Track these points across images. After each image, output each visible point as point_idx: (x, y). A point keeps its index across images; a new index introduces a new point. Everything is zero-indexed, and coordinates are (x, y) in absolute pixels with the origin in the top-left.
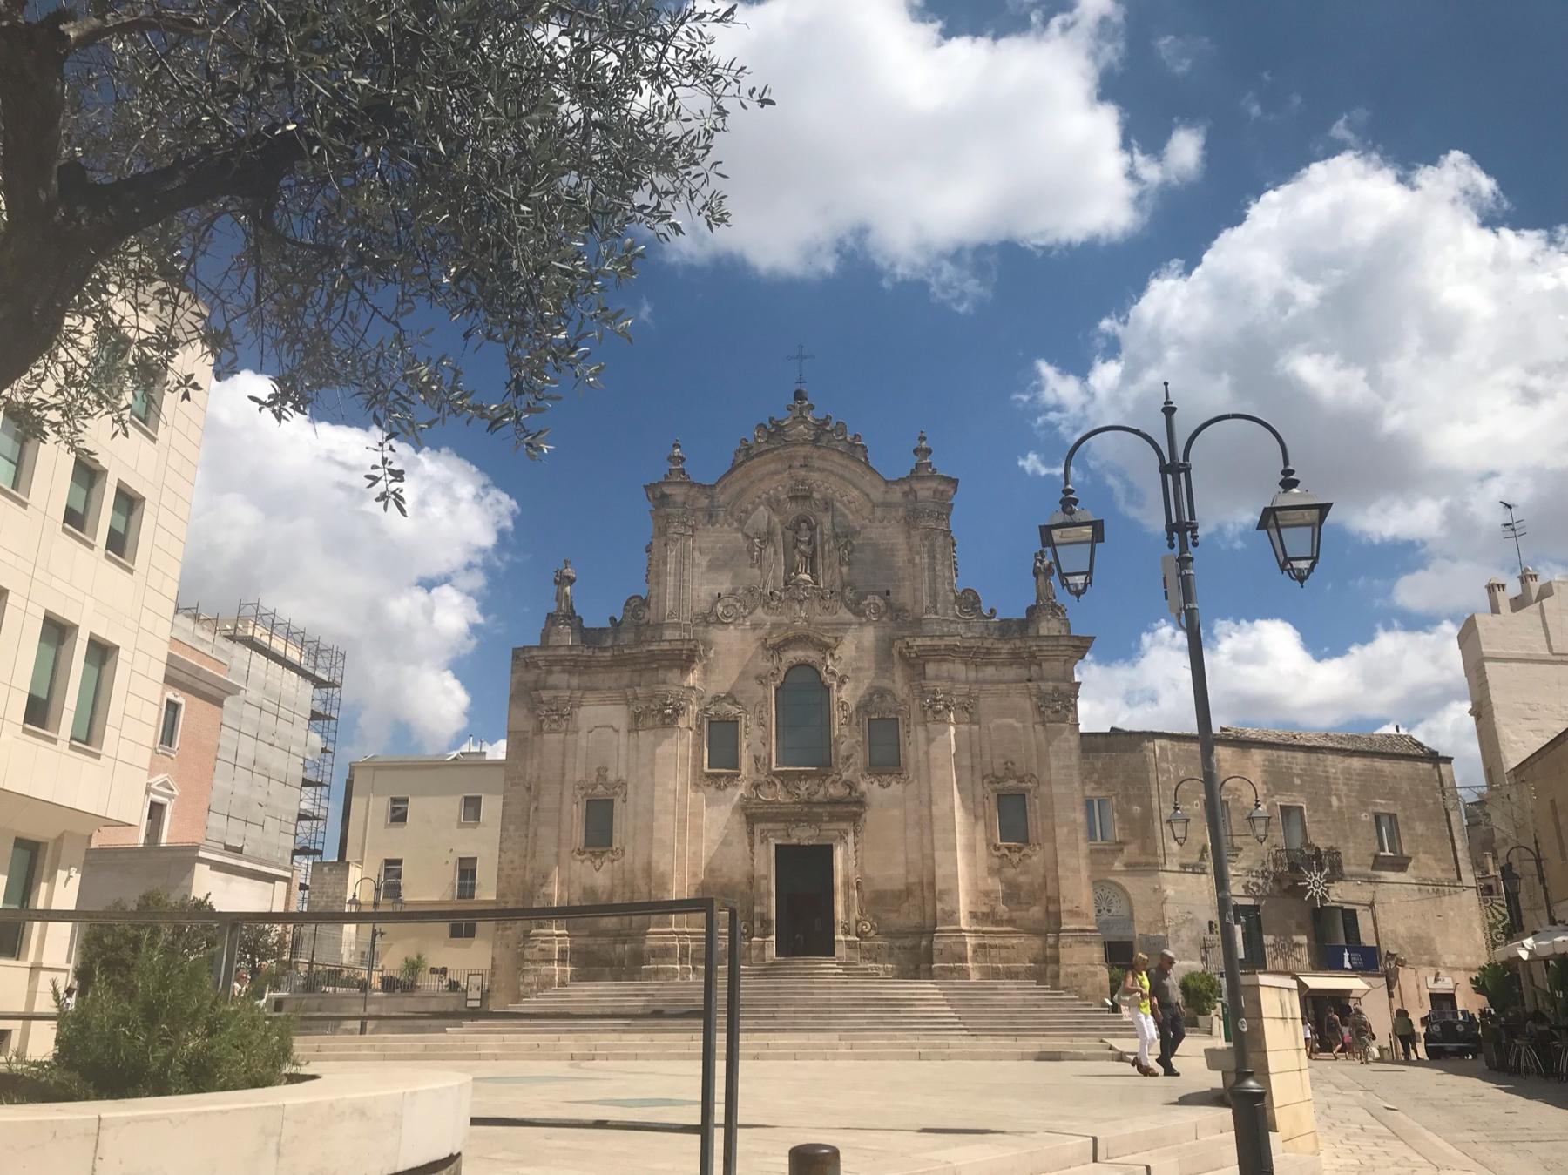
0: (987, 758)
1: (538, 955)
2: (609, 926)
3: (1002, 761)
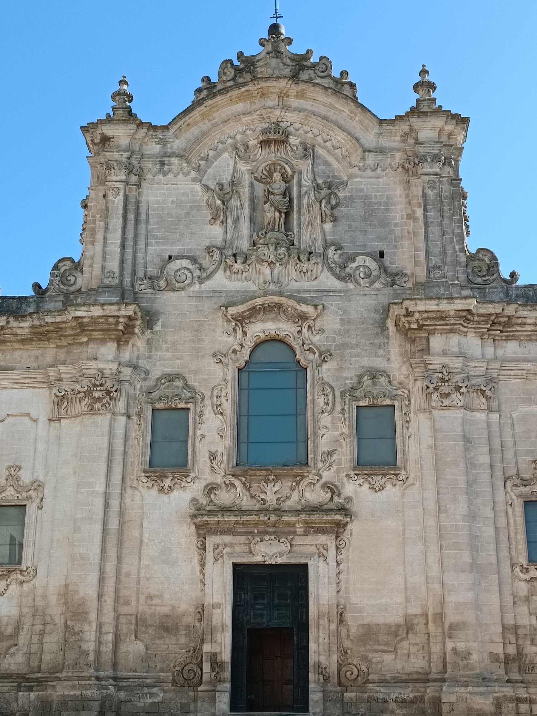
0: (509, 455)
2: (13, 667)
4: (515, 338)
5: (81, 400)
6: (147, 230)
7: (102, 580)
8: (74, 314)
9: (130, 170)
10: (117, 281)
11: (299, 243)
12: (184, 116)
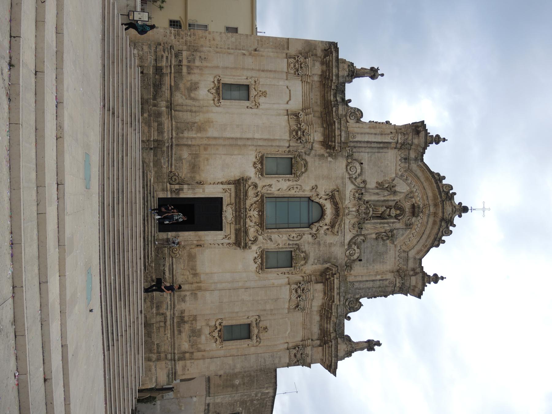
1: (159, 54)
2: (176, 97)
3: (268, 326)
4: (321, 319)
5: (297, 126)
6: (374, 153)
7: (215, 138)
8: (336, 121)
9: (403, 144)
10: (351, 140)
11: (367, 223)
12: (427, 169)
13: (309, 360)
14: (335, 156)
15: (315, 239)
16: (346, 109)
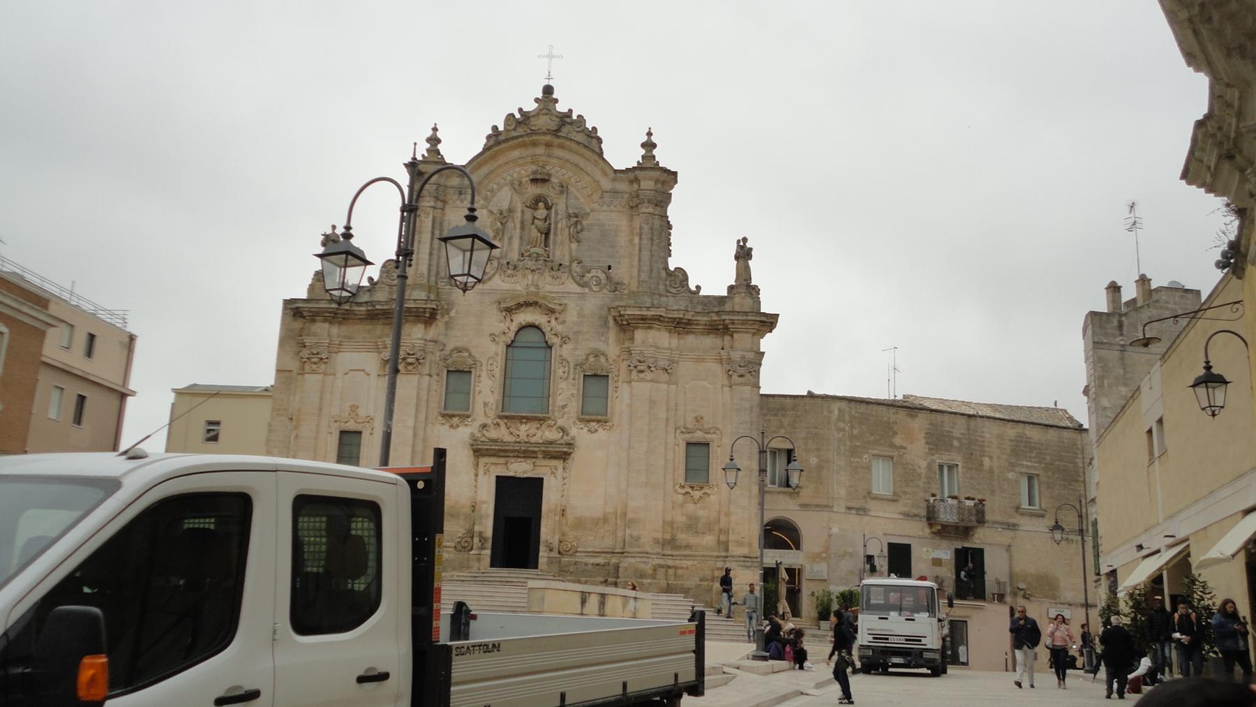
4: (692, 333)
9: (437, 198)
10: (426, 280)
11: (553, 257)
13: (750, 356)
14: (448, 304)
15: (569, 339)
16: (382, 286)
